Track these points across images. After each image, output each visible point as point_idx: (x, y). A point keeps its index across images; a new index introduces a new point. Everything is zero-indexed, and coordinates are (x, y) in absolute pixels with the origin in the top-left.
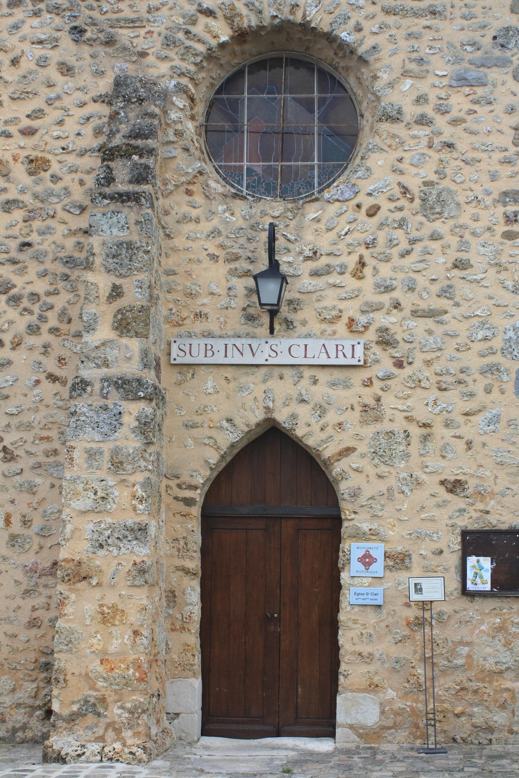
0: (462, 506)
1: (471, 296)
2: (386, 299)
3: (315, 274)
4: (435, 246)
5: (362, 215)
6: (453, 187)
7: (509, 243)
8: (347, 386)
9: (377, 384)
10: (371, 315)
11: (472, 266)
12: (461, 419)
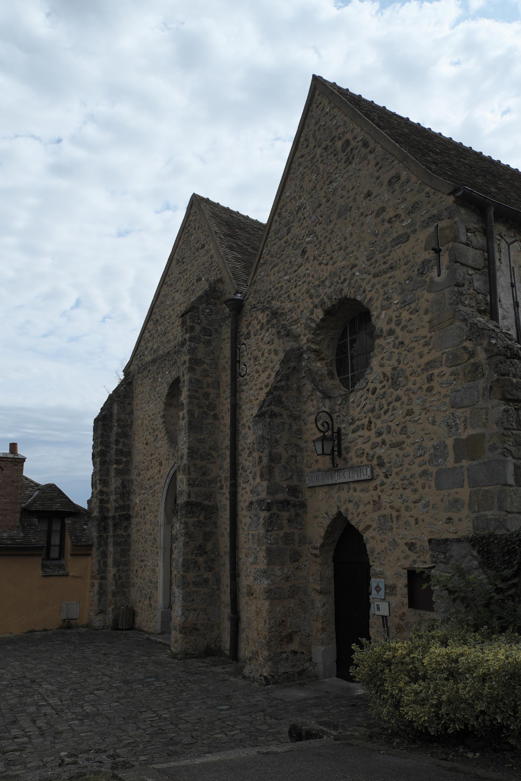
0: (415, 558)
1: (414, 431)
2: (379, 440)
3: (354, 432)
4: (398, 404)
5: (370, 395)
6: (405, 367)
7: (429, 394)
8: (367, 491)
9: (379, 488)
10: (375, 450)
11: (414, 413)
12: (412, 505)
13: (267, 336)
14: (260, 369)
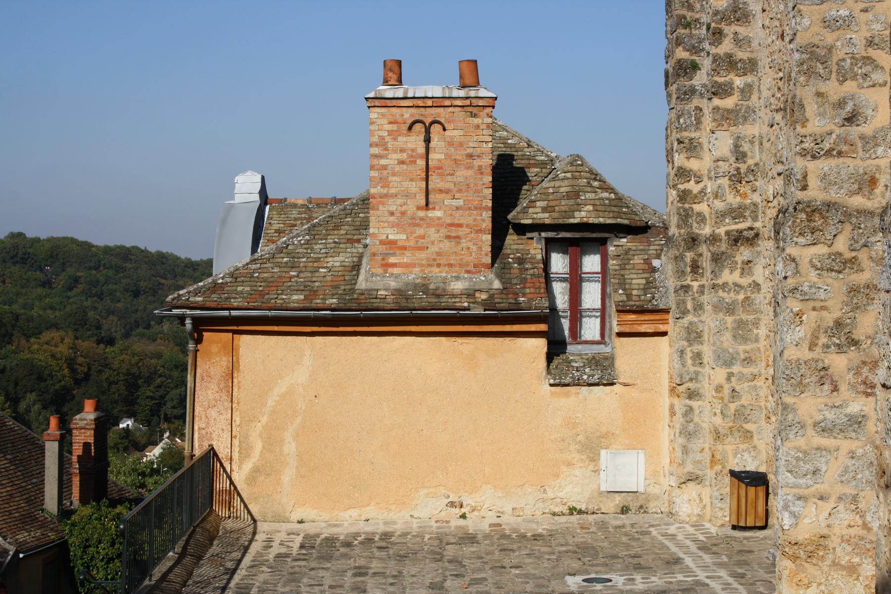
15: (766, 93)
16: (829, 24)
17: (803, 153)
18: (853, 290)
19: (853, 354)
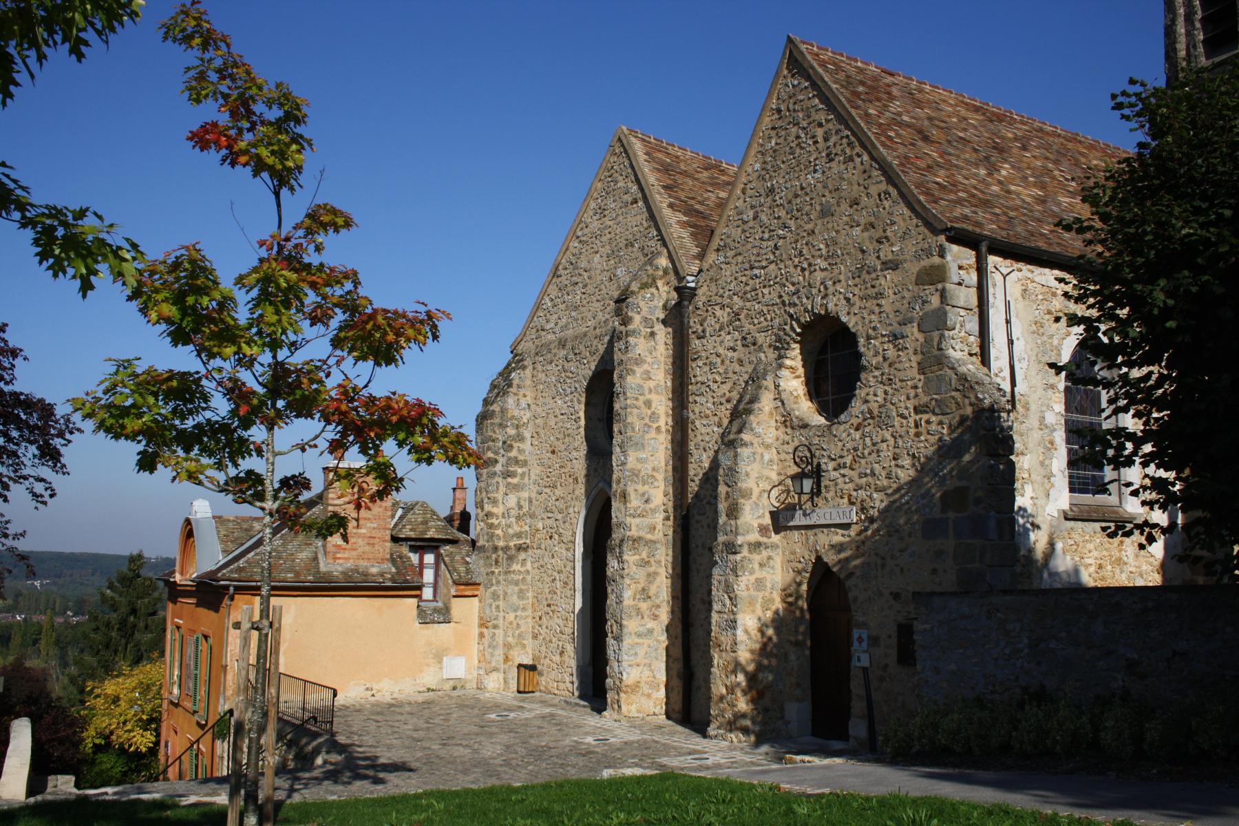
4: (884, 445)
13: (728, 340)
14: (718, 378)
15: (533, 477)
16: (639, 460)
17: (630, 515)
18: (649, 575)
19: (649, 602)
